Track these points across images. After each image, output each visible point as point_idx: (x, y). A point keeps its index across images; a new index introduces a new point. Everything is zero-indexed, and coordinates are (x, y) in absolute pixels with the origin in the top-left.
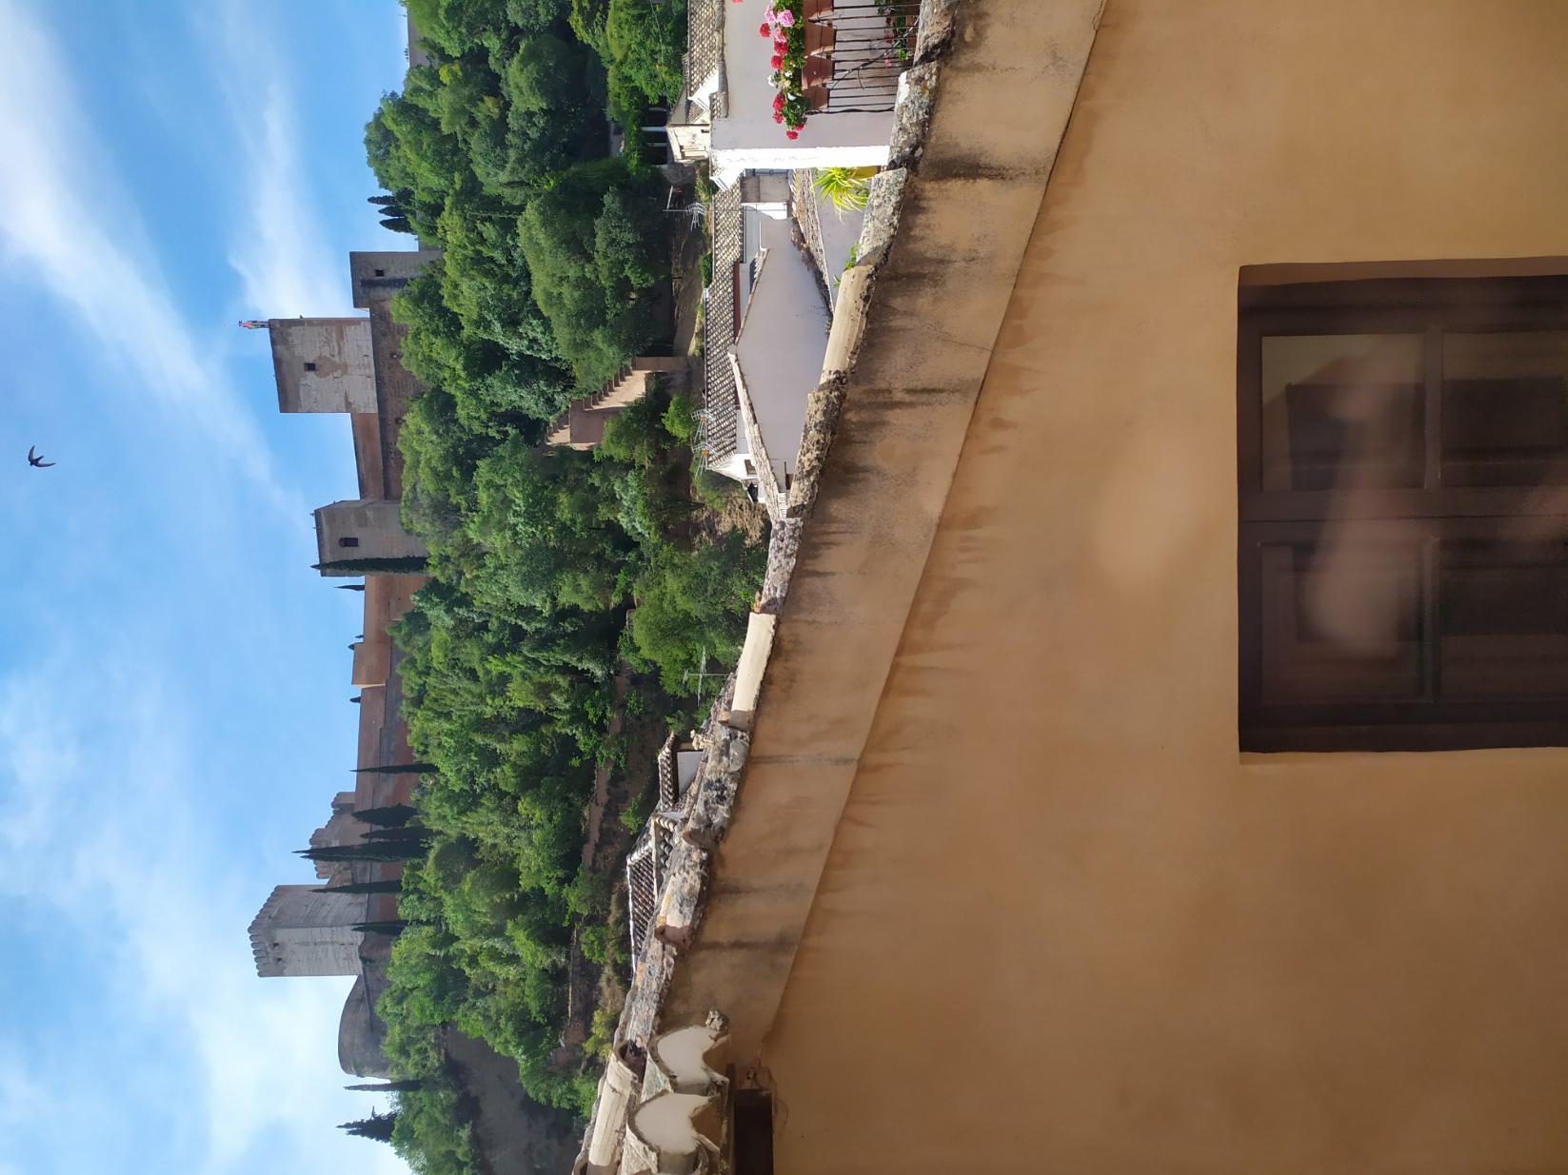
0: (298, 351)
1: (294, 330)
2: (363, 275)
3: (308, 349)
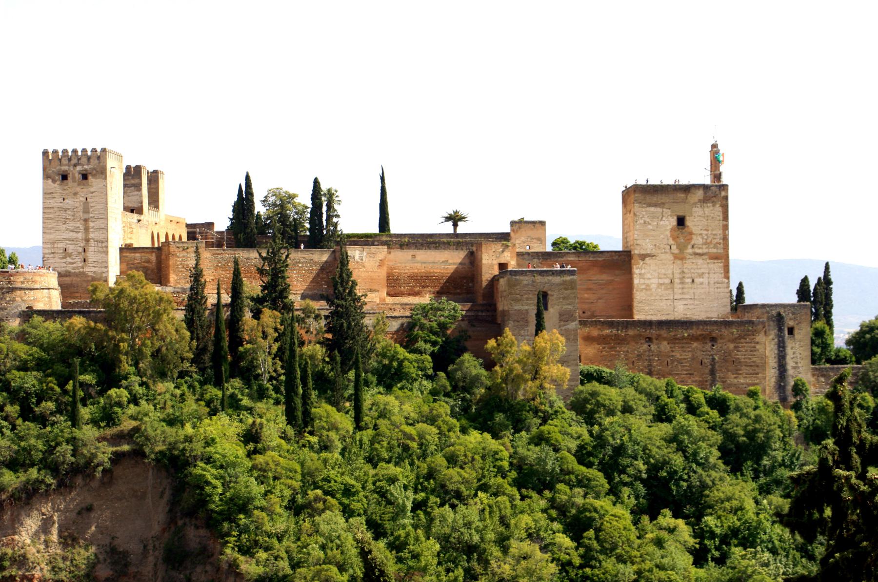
0: (698, 211)
1: (718, 209)
3: (699, 219)
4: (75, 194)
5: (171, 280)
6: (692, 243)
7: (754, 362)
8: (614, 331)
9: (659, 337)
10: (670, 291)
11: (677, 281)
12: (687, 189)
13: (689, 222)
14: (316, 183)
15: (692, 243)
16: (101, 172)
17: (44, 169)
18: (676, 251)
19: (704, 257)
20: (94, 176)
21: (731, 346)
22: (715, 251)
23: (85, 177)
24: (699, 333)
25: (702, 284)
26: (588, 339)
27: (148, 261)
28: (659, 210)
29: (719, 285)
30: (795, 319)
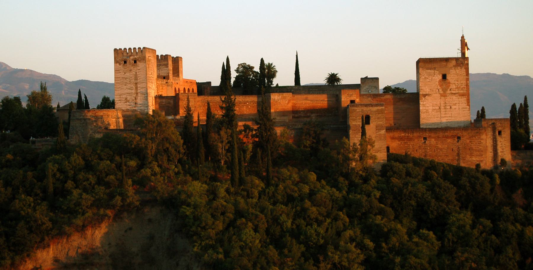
0: (453, 71)
1: (463, 70)
2: (498, 125)
4: (131, 70)
5: (180, 112)
8: (407, 135)
9: (430, 137)
10: (439, 113)
11: (442, 107)
12: (447, 60)
13: (448, 77)
14: (262, 60)
16: (143, 59)
17: (115, 59)
20: (140, 61)
21: (468, 141)
22: (462, 92)
23: (135, 62)
24: (451, 134)
25: (455, 109)
26: (393, 138)
27: (169, 103)
28: (432, 71)
29: (463, 109)
30: (502, 126)
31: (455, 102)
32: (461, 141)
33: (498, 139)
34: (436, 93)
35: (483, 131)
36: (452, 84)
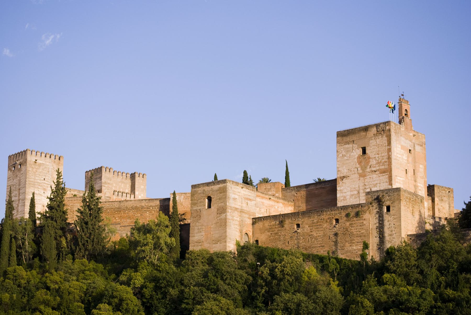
0: (373, 142)
1: (385, 138)
6: (370, 164)
7: (362, 233)
12: (366, 129)
13: (367, 152)
14: (245, 173)
15: (370, 164)
18: (360, 171)
19: (376, 173)
21: (348, 224)
22: (383, 167)
28: (351, 146)
30: (390, 200)
31: (376, 182)
32: (340, 224)
33: (385, 218)
34: (355, 173)
35: (366, 208)
36: (372, 158)
